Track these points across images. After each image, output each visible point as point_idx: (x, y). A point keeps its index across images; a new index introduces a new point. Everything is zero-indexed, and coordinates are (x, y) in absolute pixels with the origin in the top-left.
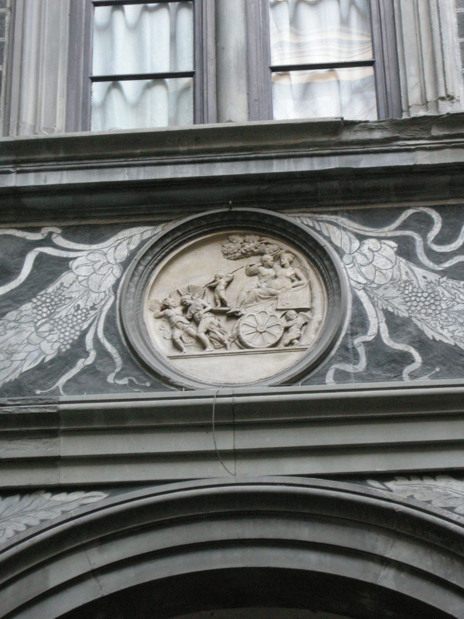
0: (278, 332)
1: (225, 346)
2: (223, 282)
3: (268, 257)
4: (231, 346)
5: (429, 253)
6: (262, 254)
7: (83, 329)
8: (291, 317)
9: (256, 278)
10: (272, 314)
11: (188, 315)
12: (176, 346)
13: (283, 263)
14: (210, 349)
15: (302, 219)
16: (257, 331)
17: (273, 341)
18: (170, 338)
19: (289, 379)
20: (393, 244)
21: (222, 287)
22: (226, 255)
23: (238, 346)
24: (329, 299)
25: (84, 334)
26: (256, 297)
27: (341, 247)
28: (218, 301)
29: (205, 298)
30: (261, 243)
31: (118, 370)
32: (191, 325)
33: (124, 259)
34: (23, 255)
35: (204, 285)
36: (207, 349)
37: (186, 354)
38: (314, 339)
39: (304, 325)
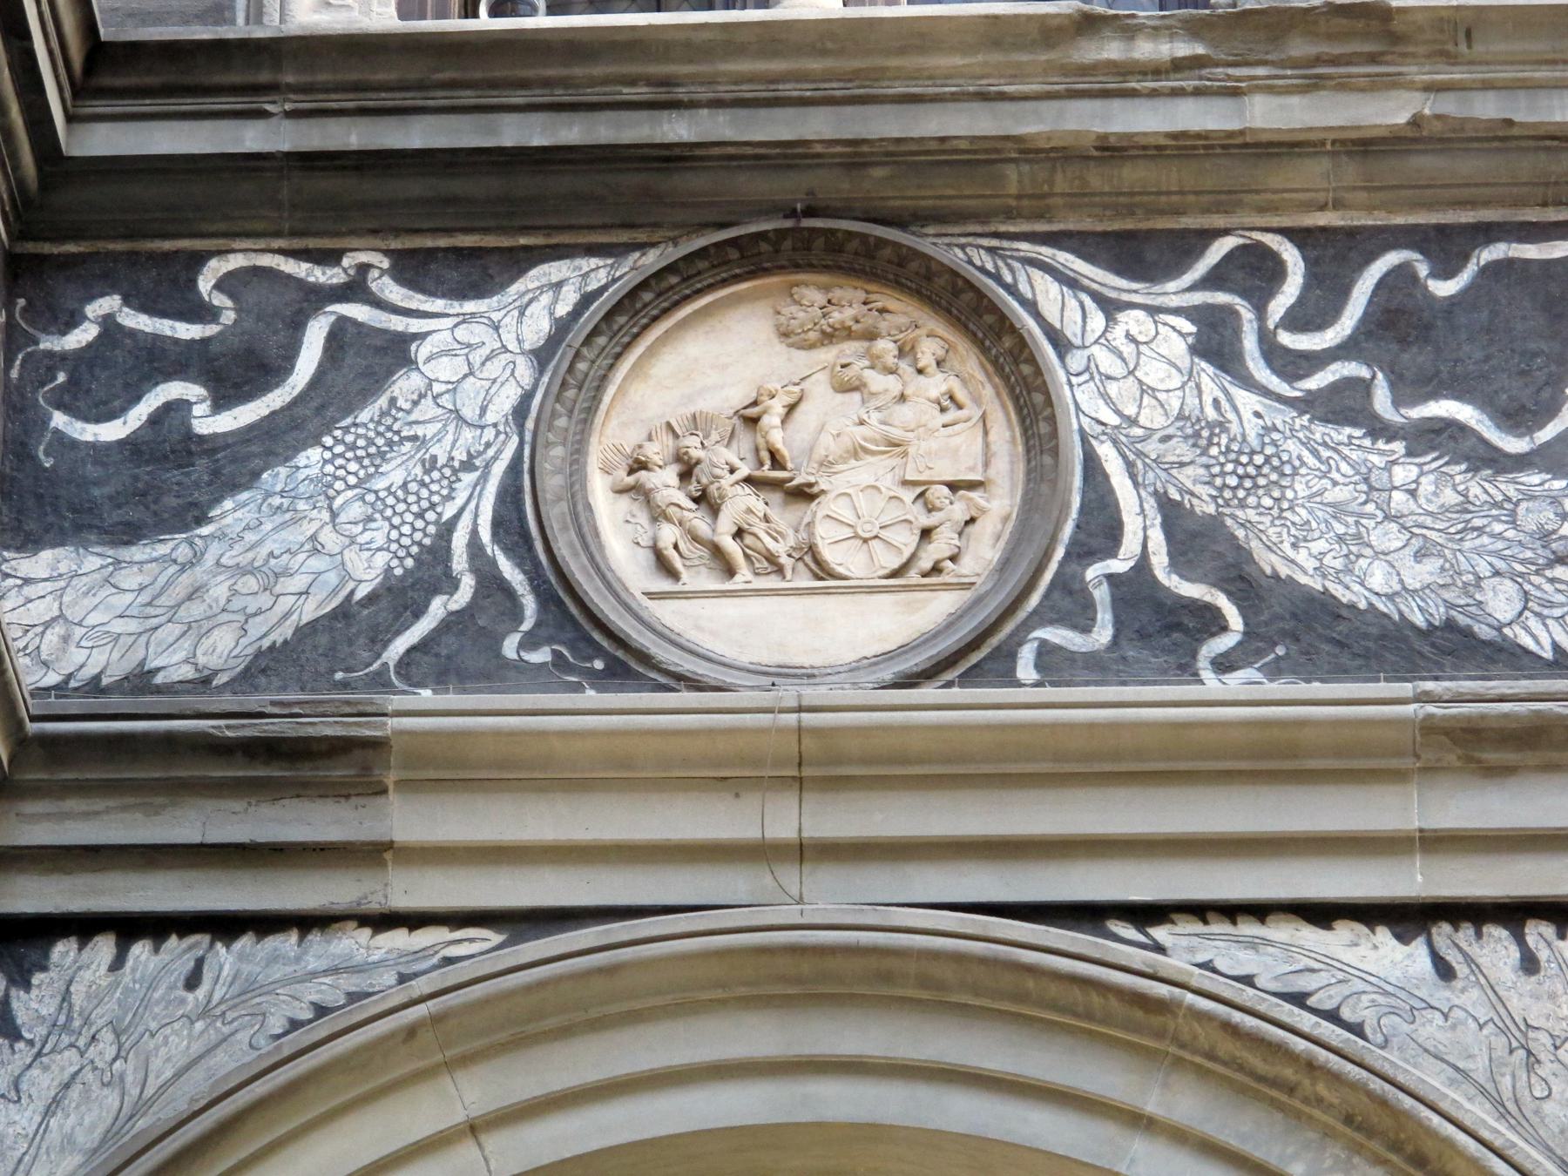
0: (906, 540)
1: (780, 570)
2: (777, 407)
3: (885, 346)
4: (793, 569)
5: (1273, 353)
6: (871, 336)
7: (445, 518)
8: (937, 503)
9: (856, 396)
10: (892, 494)
11: (693, 488)
12: (663, 565)
13: (920, 365)
14: (744, 575)
15: (970, 253)
16: (856, 536)
17: (895, 563)
18: (650, 543)
19: (928, 665)
20: (1188, 327)
21: (777, 421)
22: (785, 334)
23: (811, 570)
24: (1029, 461)
25: (447, 529)
26: (855, 449)
27: (1062, 331)
28: (765, 455)
29: (734, 445)
30: (870, 310)
31: (527, 626)
32: (699, 514)
33: (542, 342)
34: (297, 326)
35: (732, 411)
36: (738, 578)
37: (686, 588)
38: (991, 561)
39: (967, 523)
